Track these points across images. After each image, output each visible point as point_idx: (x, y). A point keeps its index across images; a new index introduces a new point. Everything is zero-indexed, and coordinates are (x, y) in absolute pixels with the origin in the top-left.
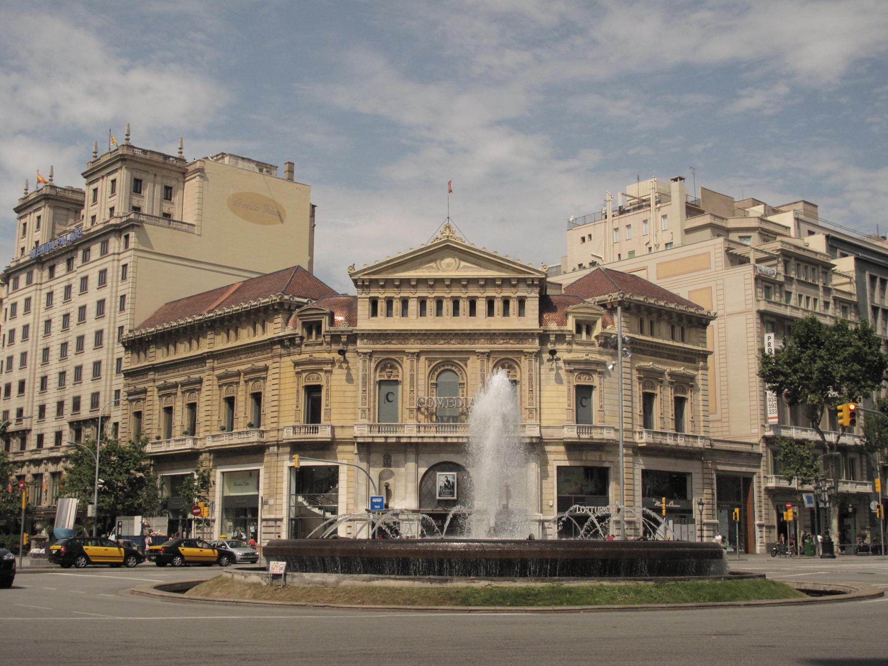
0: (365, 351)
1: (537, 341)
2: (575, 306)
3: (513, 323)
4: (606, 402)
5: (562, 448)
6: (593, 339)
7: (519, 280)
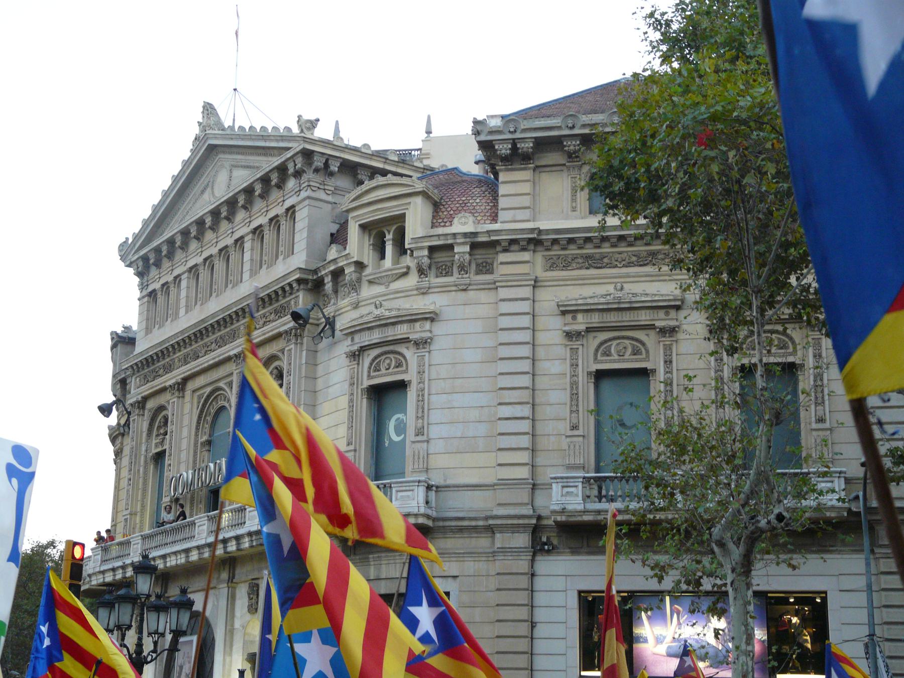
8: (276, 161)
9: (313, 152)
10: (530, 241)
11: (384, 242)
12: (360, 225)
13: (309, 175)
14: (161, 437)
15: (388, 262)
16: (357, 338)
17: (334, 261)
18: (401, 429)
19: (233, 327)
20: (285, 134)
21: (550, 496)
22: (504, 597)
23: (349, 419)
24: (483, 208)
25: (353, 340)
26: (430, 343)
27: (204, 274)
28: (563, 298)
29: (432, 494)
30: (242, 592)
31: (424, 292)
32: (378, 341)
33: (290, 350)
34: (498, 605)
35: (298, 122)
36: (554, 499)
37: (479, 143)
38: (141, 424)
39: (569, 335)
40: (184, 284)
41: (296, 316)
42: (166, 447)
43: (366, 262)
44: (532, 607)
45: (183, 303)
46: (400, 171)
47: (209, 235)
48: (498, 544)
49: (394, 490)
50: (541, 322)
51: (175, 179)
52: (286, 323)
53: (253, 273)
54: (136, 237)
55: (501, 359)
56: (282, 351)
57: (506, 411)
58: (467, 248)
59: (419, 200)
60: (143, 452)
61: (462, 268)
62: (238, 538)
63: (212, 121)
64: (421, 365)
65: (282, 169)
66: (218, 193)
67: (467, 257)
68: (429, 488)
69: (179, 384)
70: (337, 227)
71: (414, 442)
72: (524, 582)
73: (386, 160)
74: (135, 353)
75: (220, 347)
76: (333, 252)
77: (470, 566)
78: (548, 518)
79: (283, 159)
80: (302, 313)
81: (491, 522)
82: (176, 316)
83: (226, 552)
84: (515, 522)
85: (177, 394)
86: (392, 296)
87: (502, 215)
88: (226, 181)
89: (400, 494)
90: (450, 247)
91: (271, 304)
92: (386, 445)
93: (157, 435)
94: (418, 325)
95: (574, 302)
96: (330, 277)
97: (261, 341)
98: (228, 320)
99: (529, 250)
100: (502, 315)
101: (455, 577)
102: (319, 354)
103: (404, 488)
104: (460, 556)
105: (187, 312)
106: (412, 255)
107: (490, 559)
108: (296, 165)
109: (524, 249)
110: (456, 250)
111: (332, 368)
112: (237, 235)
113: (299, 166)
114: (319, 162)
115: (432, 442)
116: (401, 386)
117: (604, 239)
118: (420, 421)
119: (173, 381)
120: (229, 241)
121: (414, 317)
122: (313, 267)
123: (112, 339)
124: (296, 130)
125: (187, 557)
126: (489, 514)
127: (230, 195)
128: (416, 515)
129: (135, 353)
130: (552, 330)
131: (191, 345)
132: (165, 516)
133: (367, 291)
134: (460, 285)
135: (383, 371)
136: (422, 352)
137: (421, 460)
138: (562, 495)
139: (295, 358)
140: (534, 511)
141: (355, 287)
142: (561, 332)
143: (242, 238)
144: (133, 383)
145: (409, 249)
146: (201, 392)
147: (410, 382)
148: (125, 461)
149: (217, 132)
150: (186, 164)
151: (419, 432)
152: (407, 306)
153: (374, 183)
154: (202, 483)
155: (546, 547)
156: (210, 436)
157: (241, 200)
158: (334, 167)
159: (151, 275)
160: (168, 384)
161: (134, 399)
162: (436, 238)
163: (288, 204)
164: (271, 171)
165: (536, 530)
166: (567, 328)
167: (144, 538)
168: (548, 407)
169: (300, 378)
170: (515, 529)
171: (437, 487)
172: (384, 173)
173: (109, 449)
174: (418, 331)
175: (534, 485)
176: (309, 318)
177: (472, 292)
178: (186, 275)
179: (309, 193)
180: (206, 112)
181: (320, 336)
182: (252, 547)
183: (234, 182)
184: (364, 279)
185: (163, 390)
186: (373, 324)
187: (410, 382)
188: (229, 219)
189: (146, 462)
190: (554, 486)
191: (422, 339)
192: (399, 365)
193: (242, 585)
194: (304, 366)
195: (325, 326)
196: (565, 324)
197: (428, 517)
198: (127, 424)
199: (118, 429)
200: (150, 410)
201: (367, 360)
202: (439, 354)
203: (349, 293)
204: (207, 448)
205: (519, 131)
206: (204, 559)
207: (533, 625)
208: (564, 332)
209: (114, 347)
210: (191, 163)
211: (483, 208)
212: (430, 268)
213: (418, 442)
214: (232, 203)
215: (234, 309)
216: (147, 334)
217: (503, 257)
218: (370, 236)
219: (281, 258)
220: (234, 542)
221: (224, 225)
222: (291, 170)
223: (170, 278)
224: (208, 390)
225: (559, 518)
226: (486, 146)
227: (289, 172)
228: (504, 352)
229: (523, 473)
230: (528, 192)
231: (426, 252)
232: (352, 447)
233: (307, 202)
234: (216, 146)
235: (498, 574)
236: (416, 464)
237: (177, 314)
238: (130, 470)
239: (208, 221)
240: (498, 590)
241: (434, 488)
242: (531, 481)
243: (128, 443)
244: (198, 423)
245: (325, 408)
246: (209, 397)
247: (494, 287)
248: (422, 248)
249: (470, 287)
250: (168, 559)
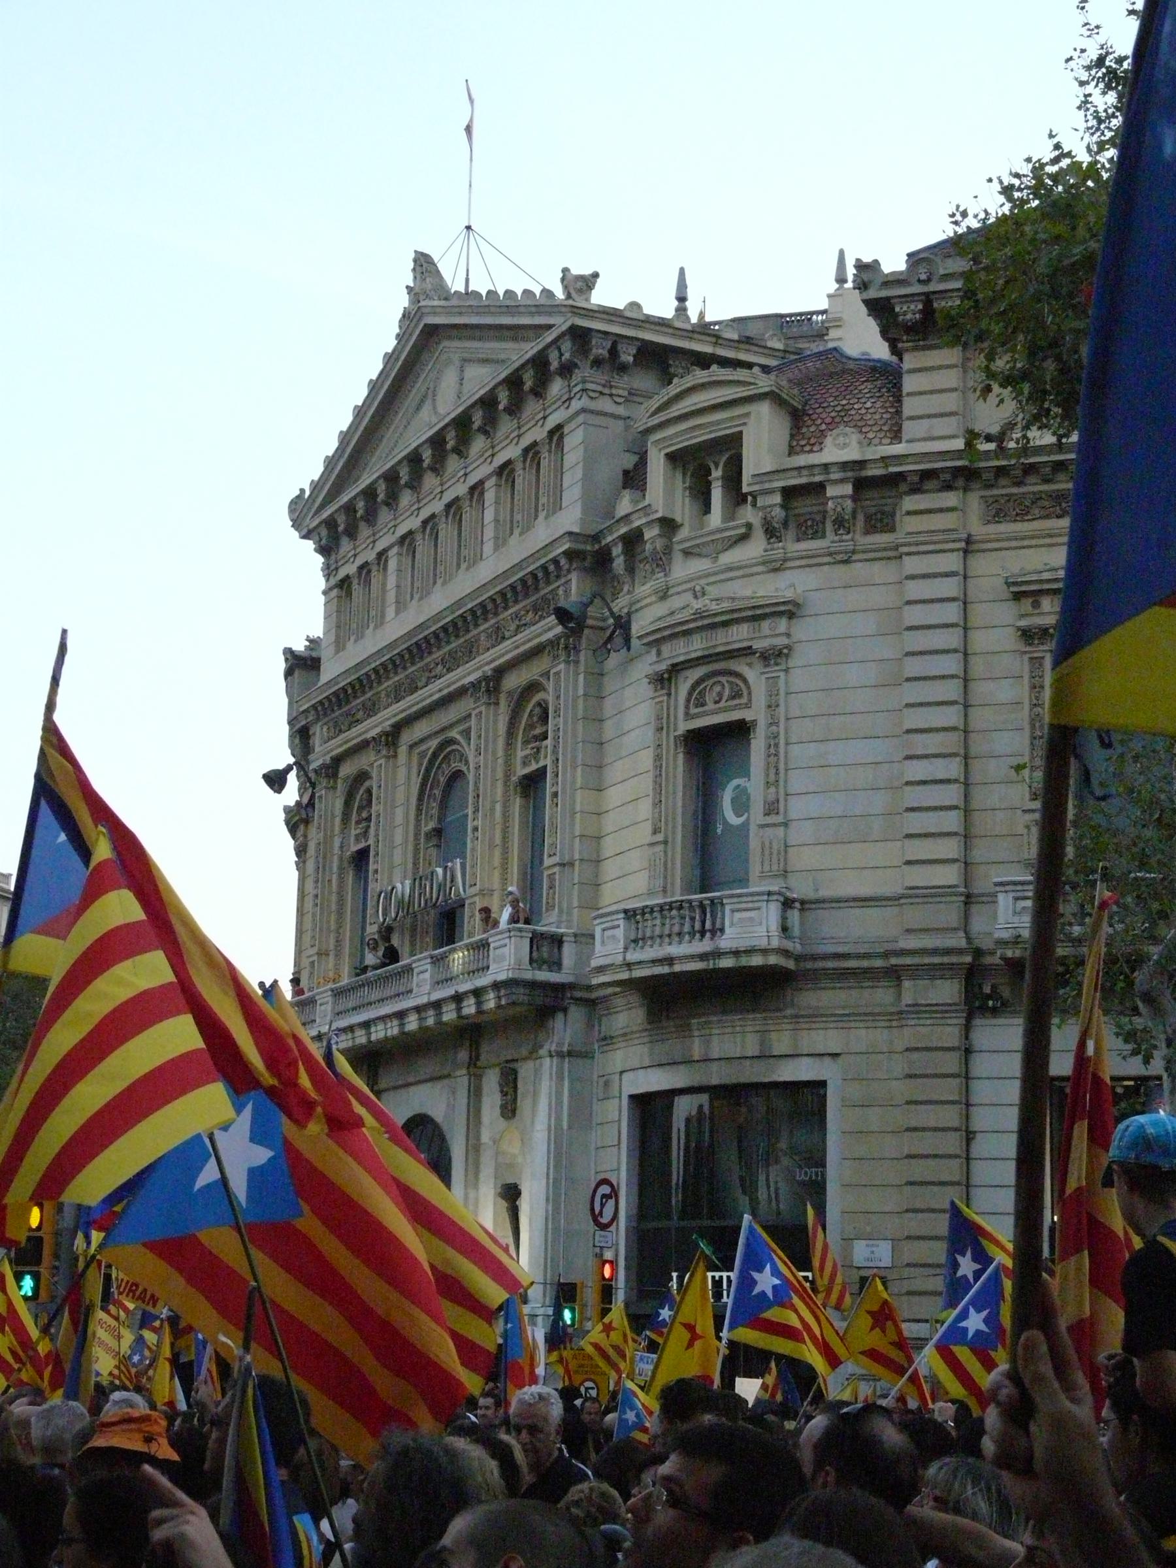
4: (797, 781)
5: (627, 1016)
8: (530, 349)
9: (590, 330)
10: (957, 472)
11: (709, 483)
13: (584, 371)
14: (364, 824)
15: (716, 517)
16: (666, 649)
17: (626, 518)
18: (741, 804)
19: (468, 637)
20: (543, 302)
21: (995, 917)
22: (919, 1089)
24: (877, 416)
25: (659, 653)
26: (787, 656)
27: (423, 546)
28: (1016, 571)
29: (794, 916)
30: (491, 1081)
31: (776, 567)
32: (699, 654)
33: (558, 673)
34: (908, 1103)
35: (563, 280)
36: (1001, 920)
37: (867, 302)
38: (332, 803)
39: (1027, 635)
40: (392, 564)
41: (563, 615)
42: (371, 841)
43: (679, 519)
44: (968, 1105)
45: (391, 596)
46: (743, 356)
47: (430, 481)
48: (907, 998)
49: (728, 908)
50: (979, 614)
51: (374, 386)
52: (549, 628)
53: (500, 543)
54: (316, 486)
55: (908, 680)
56: (546, 675)
57: (919, 770)
58: (848, 489)
59: (764, 409)
60: (336, 850)
61: (840, 523)
62: (477, 993)
63: (429, 283)
64: (773, 693)
65: (540, 363)
66: (442, 410)
67: (849, 504)
68: (787, 904)
69: (387, 734)
70: (634, 459)
71: (762, 826)
72: (951, 1062)
73: (717, 338)
74: (320, 684)
75: (449, 670)
76: (625, 505)
77: (862, 1037)
78: (992, 953)
79: (540, 347)
80: (572, 610)
81: (894, 961)
82: (381, 622)
83: (460, 1017)
84: (937, 960)
85: (384, 752)
86: (722, 577)
87: (910, 429)
88: (456, 385)
89: (738, 915)
90: (820, 487)
91: (526, 596)
92: (719, 831)
93: (358, 823)
94: (765, 624)
95: (1035, 577)
96: (620, 545)
97: (513, 659)
98: (460, 624)
99: (956, 489)
100: (909, 603)
102: (606, 679)
103: (744, 906)
104: (844, 1019)
105: (398, 612)
106: (754, 505)
107: (894, 1024)
108: (561, 355)
109: (948, 487)
110: (831, 491)
111: (628, 704)
112: (473, 479)
113: (567, 356)
114: (600, 349)
115: (793, 825)
116: (740, 730)
117: (1030, 469)
118: (772, 790)
119: (378, 730)
120: (461, 490)
121: (759, 612)
122: (592, 529)
123: (287, 660)
124: (560, 294)
125: (402, 1025)
126: (890, 946)
127: (460, 409)
128: (765, 952)
129: (320, 684)
130: (998, 629)
131: (405, 668)
132: (370, 959)
133: (682, 569)
134: (840, 553)
135: (710, 706)
136: (774, 670)
137: (775, 856)
138: (1015, 913)
139: (567, 688)
140: (969, 939)
141: (661, 561)
142: (1011, 630)
143: (481, 483)
144: (319, 732)
145: (750, 493)
146: (423, 747)
148: (310, 866)
149: (436, 303)
150: (389, 359)
151: (771, 808)
152: (748, 593)
153: (689, 381)
154: (426, 901)
155: (991, 1003)
156: (440, 820)
157: (478, 419)
158: (627, 356)
159: (342, 551)
160: (369, 735)
161: (320, 762)
162: (795, 473)
163: (551, 423)
164: (523, 366)
165: (973, 975)
166: (1023, 623)
167: (338, 993)
168: (993, 762)
169: (575, 720)
170: (935, 972)
171: (803, 902)
172: (703, 361)
173: (287, 844)
174: (767, 636)
175: (968, 896)
176: (584, 616)
177: (860, 565)
178: (395, 550)
179: (584, 402)
180: (418, 268)
181: (604, 648)
182: (499, 1007)
183: (467, 387)
184: (677, 547)
185: (364, 745)
186: (692, 625)
188: (460, 451)
189: (341, 868)
190: (1001, 897)
191: (773, 647)
192: (736, 695)
193: (487, 1071)
194: (581, 701)
195: (614, 632)
196: (1022, 616)
197: (785, 953)
198: (311, 804)
199: (298, 812)
200: (345, 780)
201: (683, 688)
202: (802, 674)
203: (653, 572)
204: (434, 841)
205: (935, 278)
206: (427, 1028)
207: (969, 1136)
208: (1019, 629)
209: (288, 673)
210: (397, 359)
211: (877, 416)
212: (785, 524)
213: (767, 825)
214: (462, 423)
215: (469, 606)
216: (337, 652)
217: (910, 503)
218: (684, 474)
219: (542, 515)
220: (472, 1000)
221: (453, 463)
222: (554, 365)
223: (371, 556)
224: (434, 744)
225: (1009, 954)
226: (880, 309)
227: (552, 368)
228: (915, 667)
229: (949, 876)
230: (954, 385)
231: (777, 499)
232: (660, 837)
233: (581, 419)
234: (436, 327)
235: (907, 1050)
236: (767, 863)
237: (383, 616)
238: (317, 882)
239: (427, 454)
240: (910, 1076)
241: (797, 905)
242: (962, 890)
243: (314, 835)
244: (420, 799)
245: (616, 771)
246: (435, 755)
247: (895, 554)
248: (771, 492)
249: (855, 557)
250: (373, 1029)
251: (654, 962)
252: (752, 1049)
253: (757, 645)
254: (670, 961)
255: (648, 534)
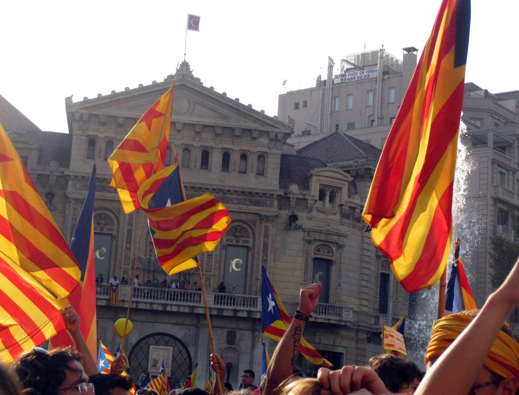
0: (77, 197)
1: (276, 203)
2: (319, 169)
3: (251, 182)
4: (344, 279)
6: (337, 209)
7: (262, 133)
12: (320, 184)
23: (305, 269)
81: (360, 328)
94: (341, 238)
101: (346, 347)
133: (314, 213)
141: (311, 210)
147: (335, 262)
149: (197, 83)
187: (335, 262)
251: (325, 319)
252: (331, 343)
253: (340, 243)
254: (329, 320)
255: (309, 202)
